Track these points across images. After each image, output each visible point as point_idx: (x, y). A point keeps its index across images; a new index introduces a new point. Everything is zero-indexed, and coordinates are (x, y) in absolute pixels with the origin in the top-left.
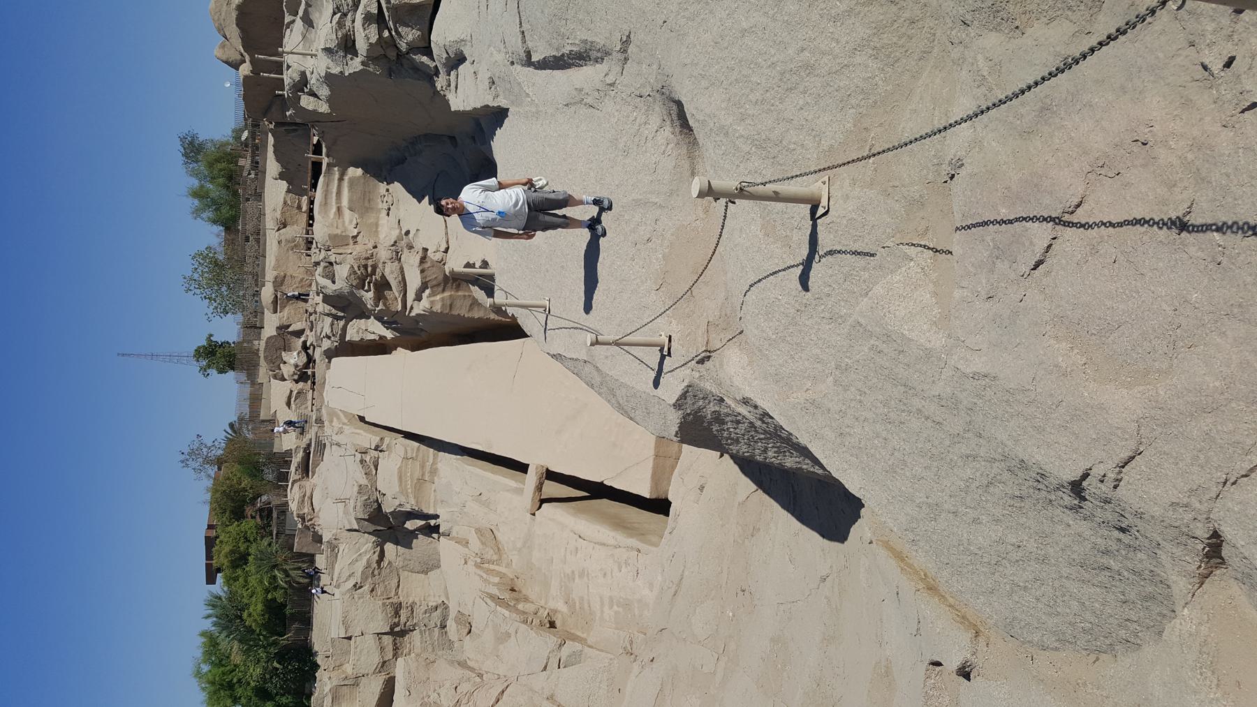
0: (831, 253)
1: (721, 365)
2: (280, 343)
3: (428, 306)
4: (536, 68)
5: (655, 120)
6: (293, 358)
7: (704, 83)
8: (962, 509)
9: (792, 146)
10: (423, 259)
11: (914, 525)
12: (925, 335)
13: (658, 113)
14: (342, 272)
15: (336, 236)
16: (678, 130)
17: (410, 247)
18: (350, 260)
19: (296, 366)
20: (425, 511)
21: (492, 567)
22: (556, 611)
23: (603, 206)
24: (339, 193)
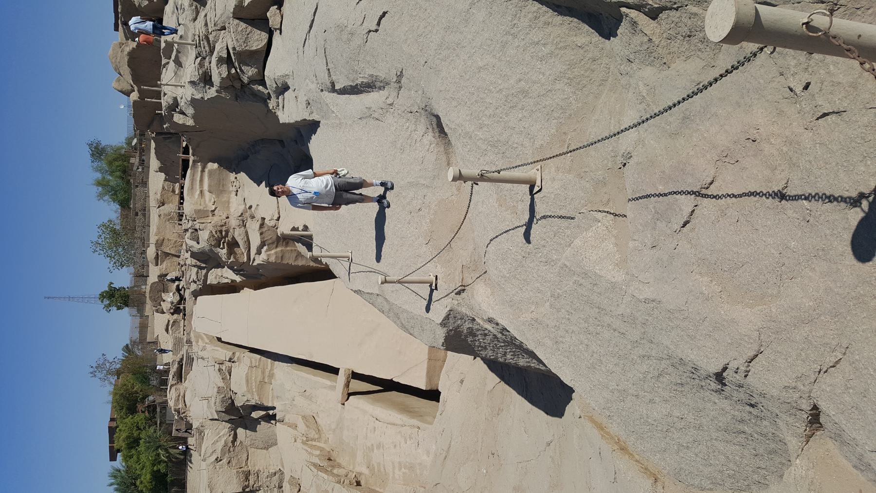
0: (544, 217)
1: (473, 296)
2: (161, 287)
3: (266, 258)
4: (339, 94)
5: (421, 128)
6: (170, 298)
7: (454, 103)
8: (641, 393)
9: (515, 145)
10: (262, 225)
11: (609, 405)
12: (612, 273)
13: (423, 124)
14: (204, 235)
15: (199, 211)
16: (437, 134)
17: (253, 217)
18: (210, 227)
19: (172, 303)
20: (266, 404)
21: (314, 443)
22: (360, 474)
23: (387, 187)
24: (201, 180)
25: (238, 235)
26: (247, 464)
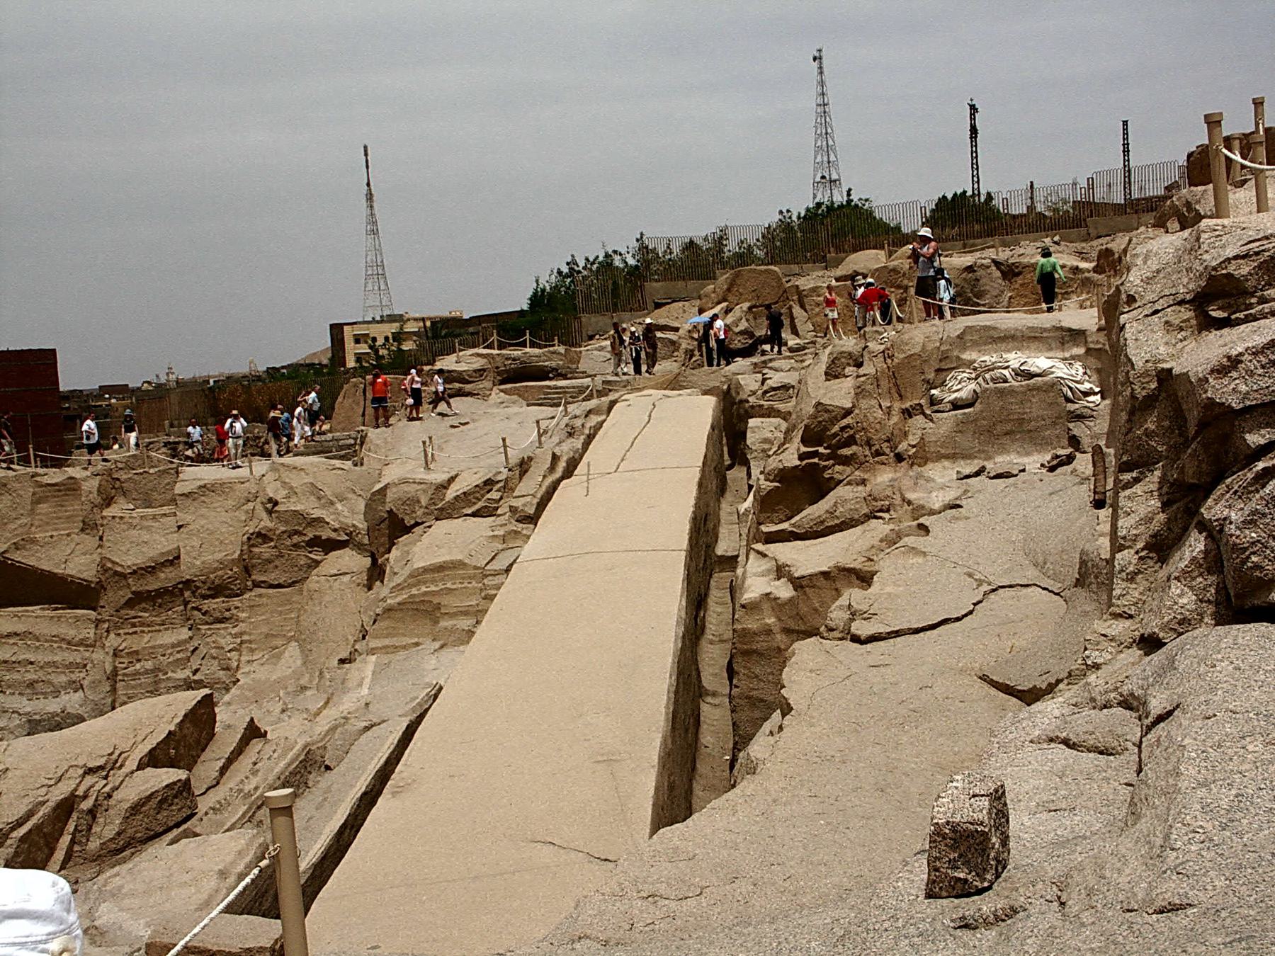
17: (891, 541)
25: (844, 497)
26: (257, 585)
